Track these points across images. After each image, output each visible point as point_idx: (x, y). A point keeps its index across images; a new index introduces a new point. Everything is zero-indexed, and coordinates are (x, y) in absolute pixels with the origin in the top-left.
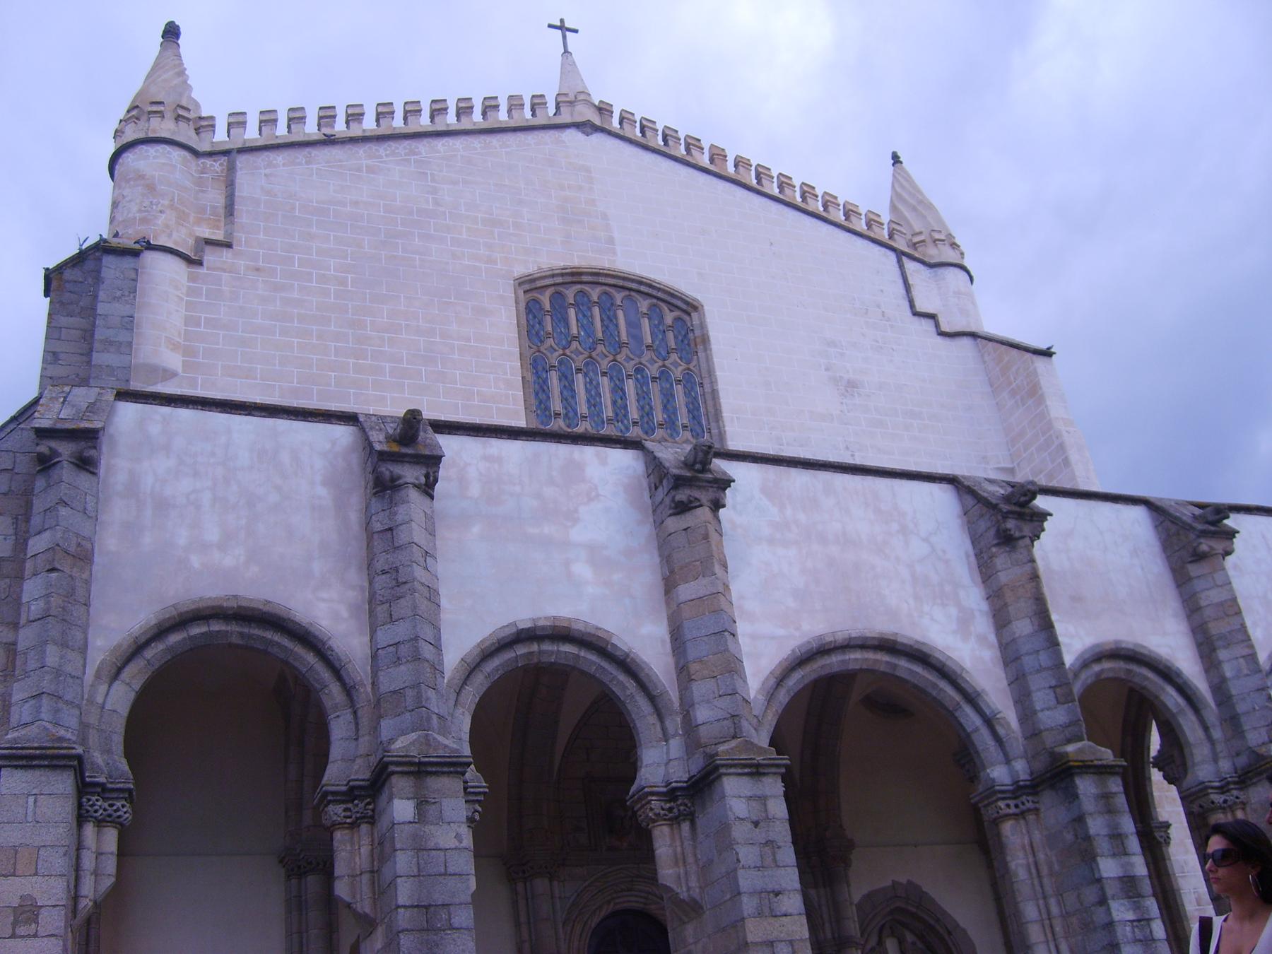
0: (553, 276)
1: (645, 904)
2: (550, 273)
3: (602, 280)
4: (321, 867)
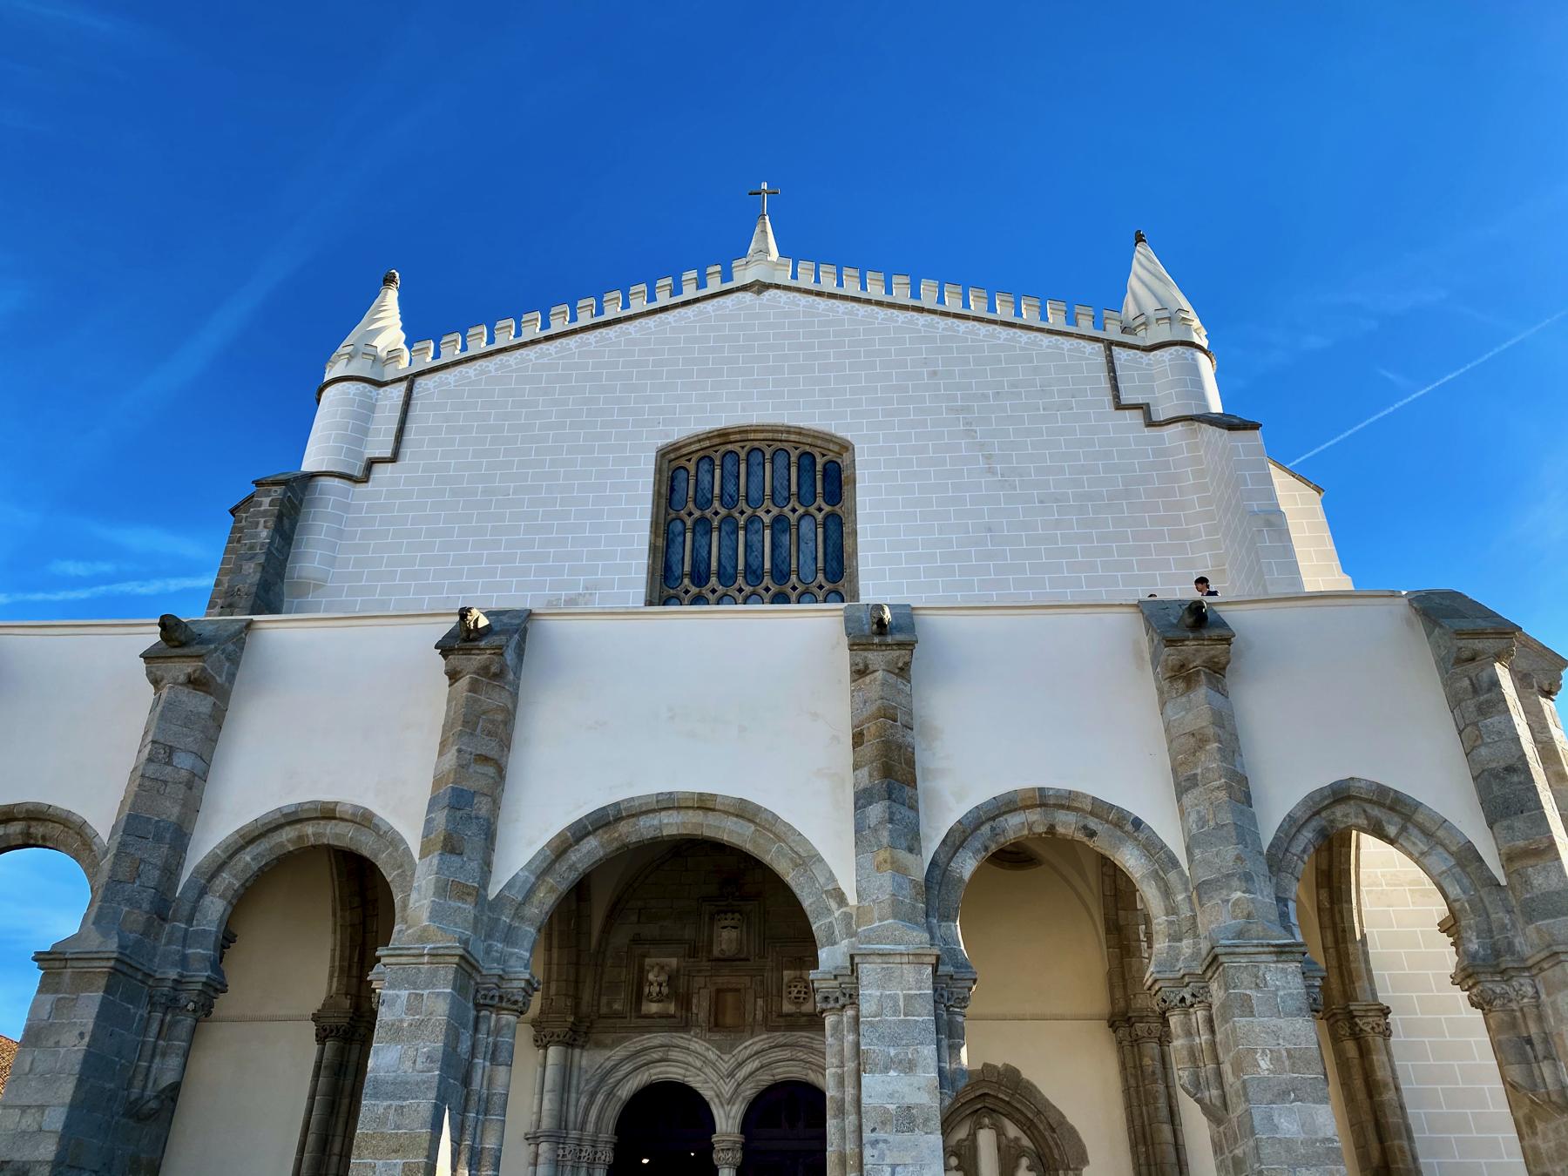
0: (699, 441)
1: (685, 1076)
2: (696, 439)
3: (752, 436)
4: (333, 1034)
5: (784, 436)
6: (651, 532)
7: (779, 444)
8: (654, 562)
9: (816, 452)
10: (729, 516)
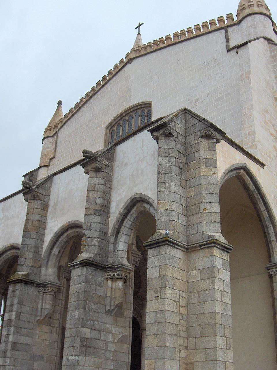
3: (128, 112)
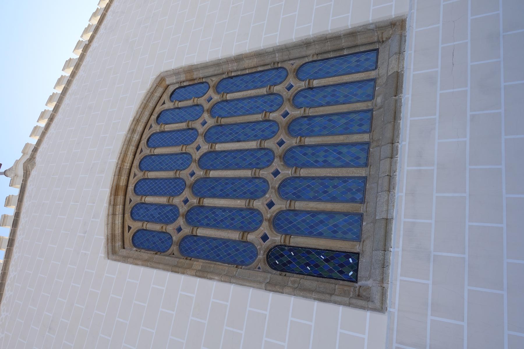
0: (114, 214)
2: (110, 217)
3: (127, 165)
5: (136, 137)
6: (183, 273)
7: (142, 142)
8: (218, 274)
9: (158, 109)
10: (192, 187)
